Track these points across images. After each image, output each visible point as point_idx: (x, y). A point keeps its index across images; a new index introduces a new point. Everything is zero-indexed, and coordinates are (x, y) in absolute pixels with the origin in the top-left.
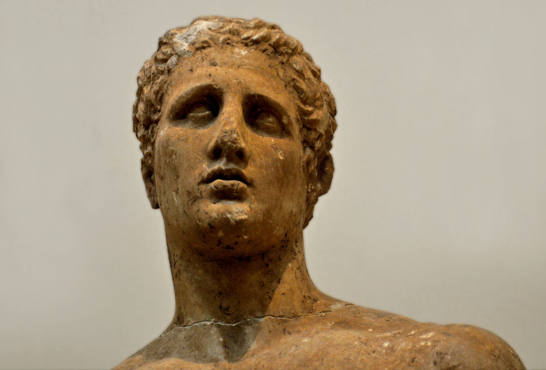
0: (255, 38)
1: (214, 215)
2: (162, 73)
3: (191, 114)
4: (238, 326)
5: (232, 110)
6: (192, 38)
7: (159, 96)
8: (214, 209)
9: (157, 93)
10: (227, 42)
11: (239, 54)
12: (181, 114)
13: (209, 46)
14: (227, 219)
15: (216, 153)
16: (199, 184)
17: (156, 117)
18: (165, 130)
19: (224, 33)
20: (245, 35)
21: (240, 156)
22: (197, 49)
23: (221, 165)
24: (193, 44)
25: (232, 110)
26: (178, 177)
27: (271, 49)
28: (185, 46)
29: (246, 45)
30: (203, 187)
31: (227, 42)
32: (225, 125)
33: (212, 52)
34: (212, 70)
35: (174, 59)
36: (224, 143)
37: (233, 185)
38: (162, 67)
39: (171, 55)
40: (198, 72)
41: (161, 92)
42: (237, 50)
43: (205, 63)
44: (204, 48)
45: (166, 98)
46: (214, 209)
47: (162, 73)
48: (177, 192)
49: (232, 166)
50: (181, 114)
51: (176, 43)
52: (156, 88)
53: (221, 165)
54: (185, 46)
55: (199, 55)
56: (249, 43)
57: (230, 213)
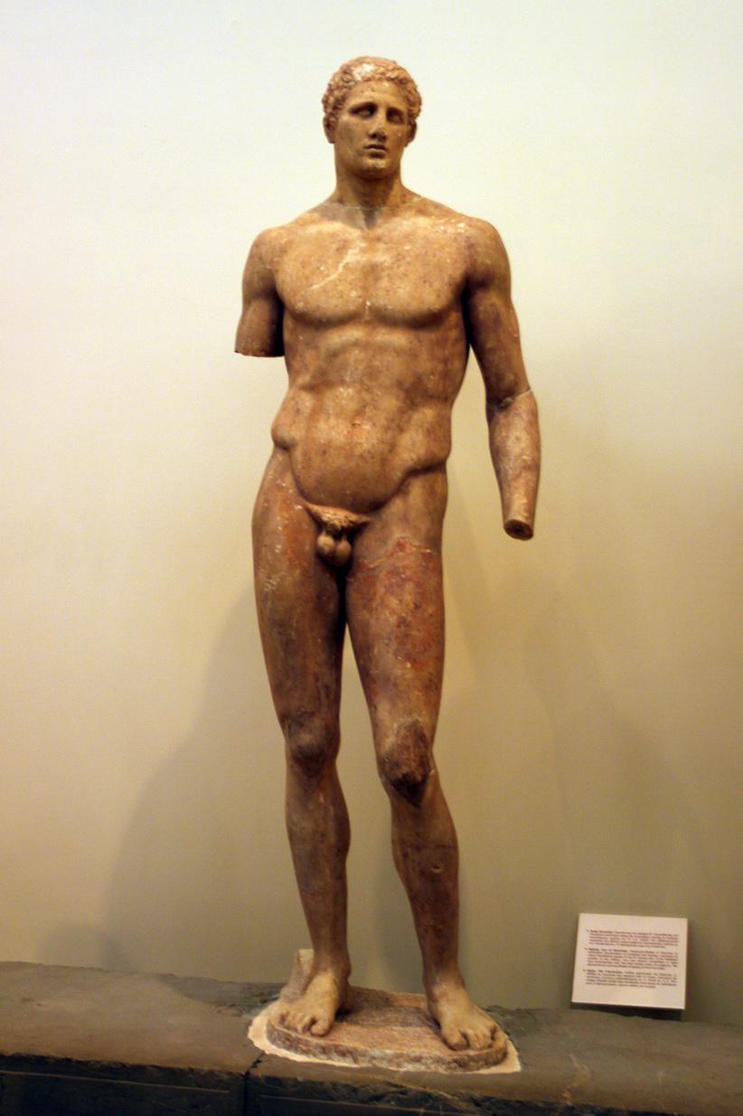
5: (381, 115)
6: (363, 75)
8: (370, 162)
10: (380, 79)
12: (356, 111)
15: (374, 136)
18: (346, 118)
21: (383, 138)
23: (374, 142)
24: (363, 77)
25: (381, 115)
28: (359, 78)
30: (366, 151)
31: (380, 79)
33: (373, 84)
34: (372, 94)
38: (345, 84)
45: (347, 101)
46: (370, 162)
49: (380, 144)
50: (356, 111)
52: (341, 94)
53: (374, 142)
55: (366, 84)
56: (390, 79)
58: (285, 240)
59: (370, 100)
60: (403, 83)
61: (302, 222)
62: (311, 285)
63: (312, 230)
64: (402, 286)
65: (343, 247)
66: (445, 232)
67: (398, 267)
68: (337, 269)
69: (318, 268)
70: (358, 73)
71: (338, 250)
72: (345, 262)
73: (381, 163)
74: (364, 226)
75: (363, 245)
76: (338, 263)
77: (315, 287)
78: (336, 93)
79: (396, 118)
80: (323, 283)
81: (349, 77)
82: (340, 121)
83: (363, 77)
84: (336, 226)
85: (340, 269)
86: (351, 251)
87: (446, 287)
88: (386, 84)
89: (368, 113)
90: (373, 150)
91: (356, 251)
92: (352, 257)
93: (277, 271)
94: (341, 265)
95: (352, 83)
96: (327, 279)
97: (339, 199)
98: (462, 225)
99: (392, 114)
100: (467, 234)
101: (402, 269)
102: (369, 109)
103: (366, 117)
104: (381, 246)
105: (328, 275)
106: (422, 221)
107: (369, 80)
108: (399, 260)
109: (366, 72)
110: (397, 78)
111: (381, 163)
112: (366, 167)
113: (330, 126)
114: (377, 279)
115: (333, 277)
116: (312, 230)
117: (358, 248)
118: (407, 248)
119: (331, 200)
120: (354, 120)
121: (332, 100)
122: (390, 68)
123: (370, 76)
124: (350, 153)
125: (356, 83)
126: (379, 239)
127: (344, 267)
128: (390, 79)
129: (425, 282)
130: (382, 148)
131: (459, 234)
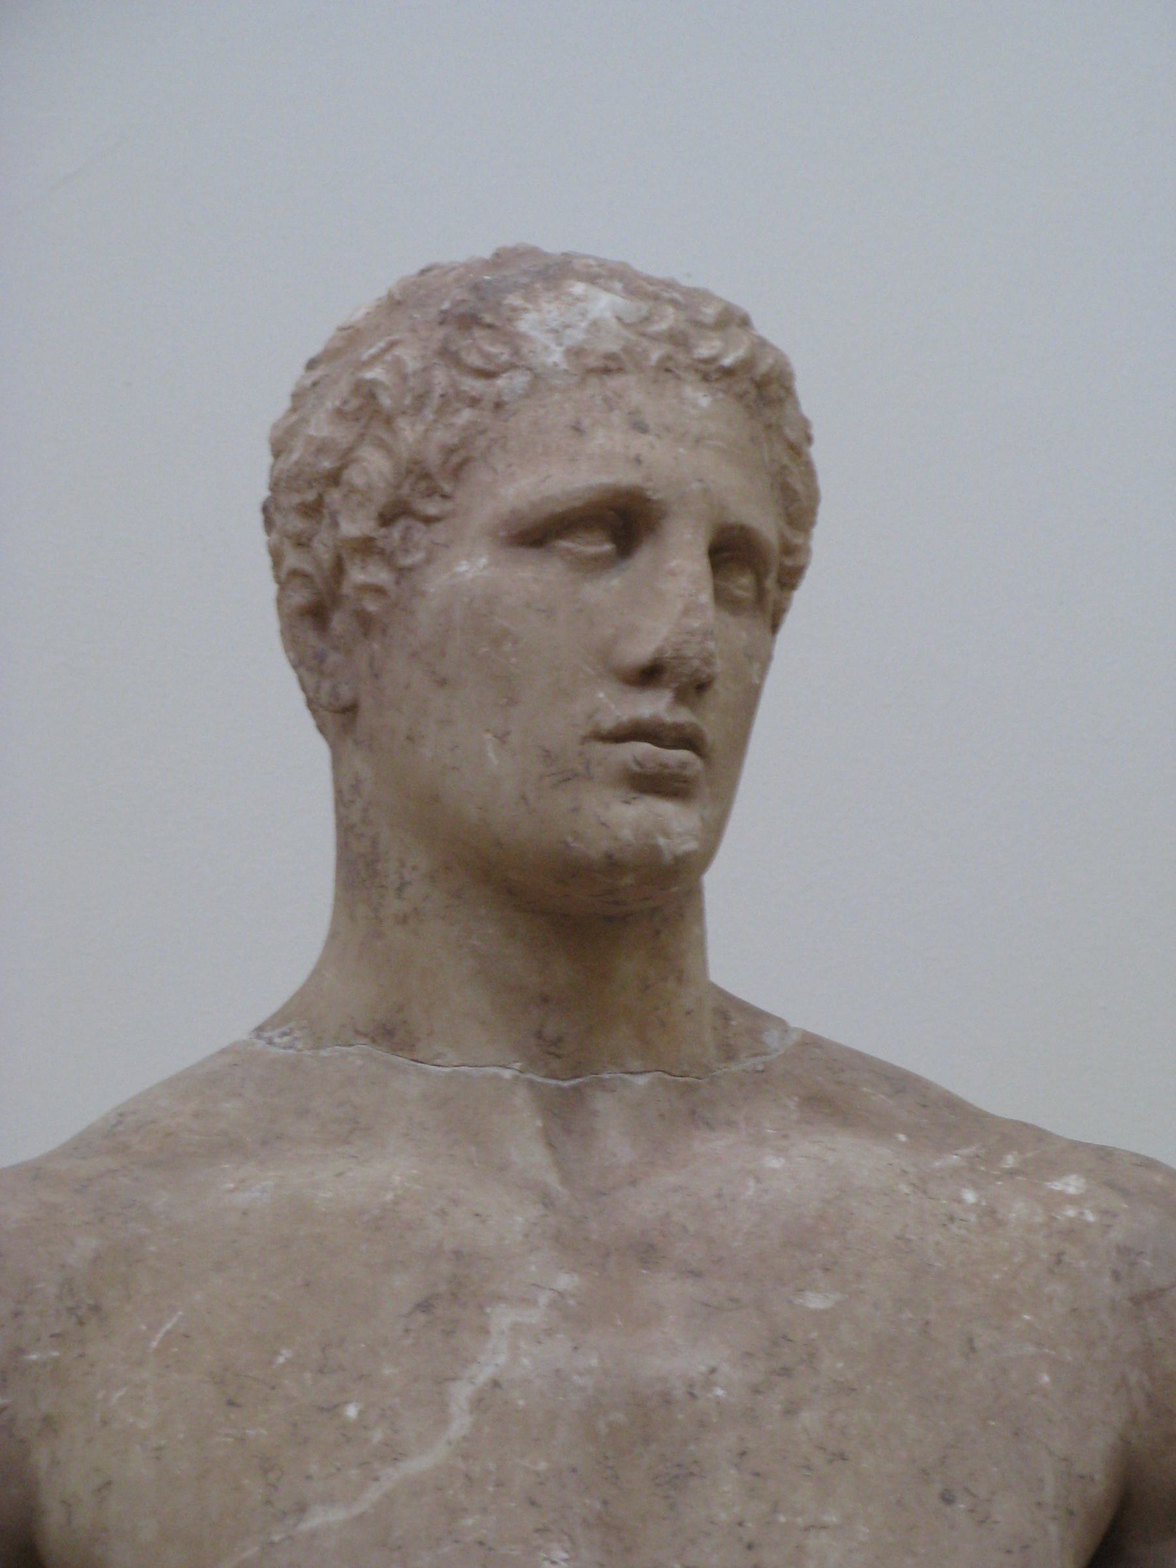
0: (727, 361)
1: (627, 834)
2: (474, 402)
3: (565, 544)
4: (576, 1089)
6: (577, 336)
7: (456, 459)
9: (450, 451)
10: (666, 368)
11: (695, 406)
12: (537, 534)
13: (620, 370)
14: (656, 850)
15: (649, 675)
16: (585, 739)
17: (432, 508)
19: (655, 338)
20: (704, 350)
22: (591, 371)
23: (654, 706)
24: (575, 353)
26: (512, 702)
27: (753, 392)
29: (706, 378)
32: (686, 612)
33: (633, 390)
34: (639, 444)
35: (520, 380)
36: (681, 659)
37: (683, 765)
39: (512, 366)
40: (599, 440)
41: (462, 453)
42: (689, 391)
43: (616, 417)
44: (607, 371)
47: (474, 402)
48: (502, 738)
49: (683, 716)
50: (537, 534)
51: (525, 337)
52: (442, 436)
53: (654, 706)
54: (556, 357)
55: (594, 388)
56: (713, 374)
57: (667, 834)
58: (88, 1244)
59: (625, 477)
60: (762, 390)
61: (140, 1146)
62: (302, 1509)
63: (248, 1189)
64: (832, 1518)
65: (454, 1297)
66: (991, 1216)
67: (791, 1410)
68: (443, 1420)
69: (333, 1410)
70: (547, 328)
71: (425, 1306)
72: (484, 1375)
73: (673, 822)
74: (552, 1179)
75: (565, 1281)
76: (442, 1380)
77: (318, 1519)
78: (409, 432)
79: (742, 584)
80: (373, 1494)
81: (501, 353)
82: (436, 583)
83: (575, 353)
84: (388, 1172)
85: (460, 1423)
86: (503, 1318)
87: (1053, 1529)
88: (703, 400)
89: (608, 547)
90: (643, 748)
91: (533, 1317)
92: (514, 1347)
93: (50, 1425)
94: (461, 1393)
95: (510, 383)
96: (391, 1477)
97: (371, 1010)
98: (1072, 1185)
99: (731, 551)
100: (1117, 1235)
101: (808, 1418)
102: (624, 522)
103: (597, 566)
104: (664, 1288)
105: (393, 1453)
106: (862, 1159)
107: (610, 367)
108: (786, 1372)
109: (595, 325)
110: (747, 365)
111: (673, 822)
112: (595, 846)
113: (325, 615)
114: (678, 1477)
115: (418, 1464)
116: (248, 1189)
117: (544, 1299)
118: (815, 1302)
119: (298, 1015)
120: (535, 577)
121: (374, 468)
122: (709, 313)
123: (612, 346)
124: (490, 765)
125: (539, 380)
126: (647, 1253)
127: (479, 1403)
128: (713, 374)
129: (947, 1498)
130: (689, 740)
131: (1072, 1232)
